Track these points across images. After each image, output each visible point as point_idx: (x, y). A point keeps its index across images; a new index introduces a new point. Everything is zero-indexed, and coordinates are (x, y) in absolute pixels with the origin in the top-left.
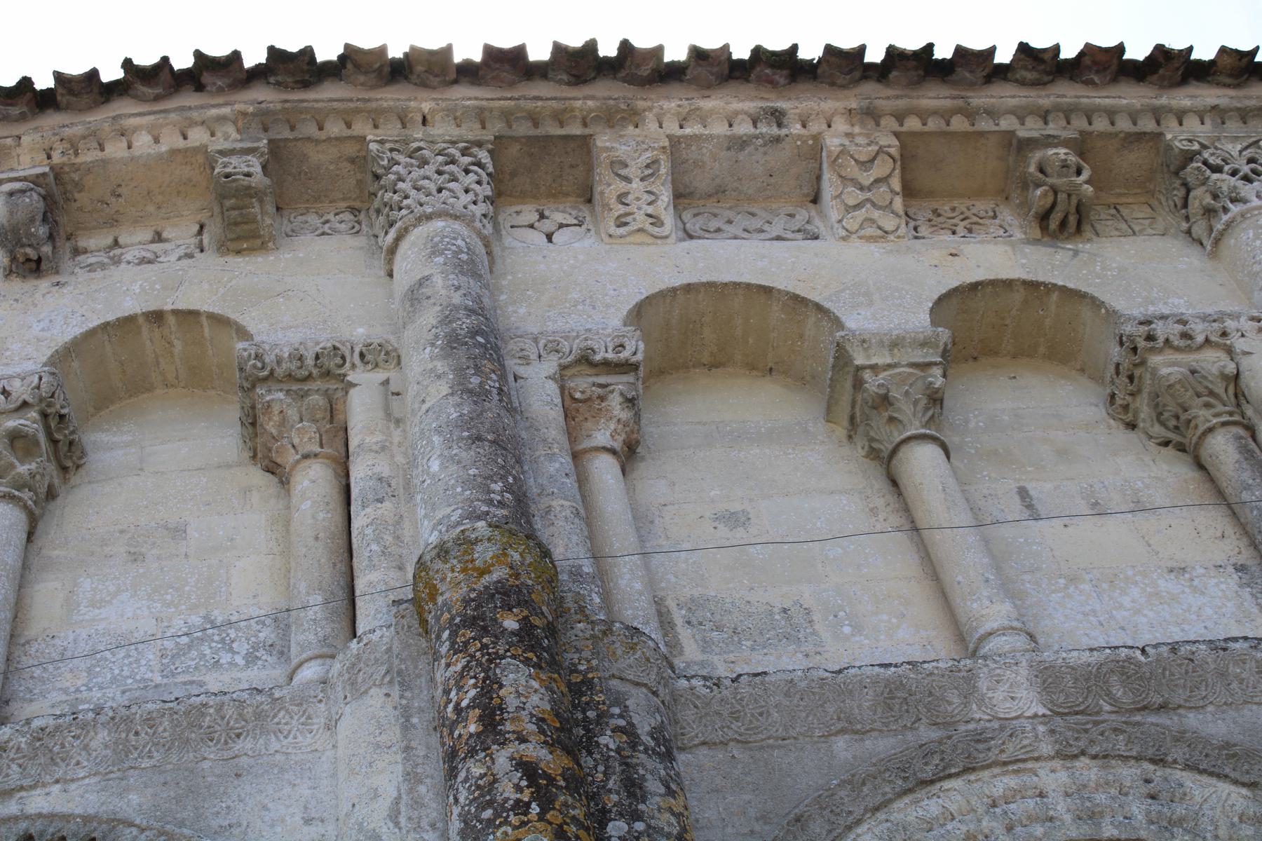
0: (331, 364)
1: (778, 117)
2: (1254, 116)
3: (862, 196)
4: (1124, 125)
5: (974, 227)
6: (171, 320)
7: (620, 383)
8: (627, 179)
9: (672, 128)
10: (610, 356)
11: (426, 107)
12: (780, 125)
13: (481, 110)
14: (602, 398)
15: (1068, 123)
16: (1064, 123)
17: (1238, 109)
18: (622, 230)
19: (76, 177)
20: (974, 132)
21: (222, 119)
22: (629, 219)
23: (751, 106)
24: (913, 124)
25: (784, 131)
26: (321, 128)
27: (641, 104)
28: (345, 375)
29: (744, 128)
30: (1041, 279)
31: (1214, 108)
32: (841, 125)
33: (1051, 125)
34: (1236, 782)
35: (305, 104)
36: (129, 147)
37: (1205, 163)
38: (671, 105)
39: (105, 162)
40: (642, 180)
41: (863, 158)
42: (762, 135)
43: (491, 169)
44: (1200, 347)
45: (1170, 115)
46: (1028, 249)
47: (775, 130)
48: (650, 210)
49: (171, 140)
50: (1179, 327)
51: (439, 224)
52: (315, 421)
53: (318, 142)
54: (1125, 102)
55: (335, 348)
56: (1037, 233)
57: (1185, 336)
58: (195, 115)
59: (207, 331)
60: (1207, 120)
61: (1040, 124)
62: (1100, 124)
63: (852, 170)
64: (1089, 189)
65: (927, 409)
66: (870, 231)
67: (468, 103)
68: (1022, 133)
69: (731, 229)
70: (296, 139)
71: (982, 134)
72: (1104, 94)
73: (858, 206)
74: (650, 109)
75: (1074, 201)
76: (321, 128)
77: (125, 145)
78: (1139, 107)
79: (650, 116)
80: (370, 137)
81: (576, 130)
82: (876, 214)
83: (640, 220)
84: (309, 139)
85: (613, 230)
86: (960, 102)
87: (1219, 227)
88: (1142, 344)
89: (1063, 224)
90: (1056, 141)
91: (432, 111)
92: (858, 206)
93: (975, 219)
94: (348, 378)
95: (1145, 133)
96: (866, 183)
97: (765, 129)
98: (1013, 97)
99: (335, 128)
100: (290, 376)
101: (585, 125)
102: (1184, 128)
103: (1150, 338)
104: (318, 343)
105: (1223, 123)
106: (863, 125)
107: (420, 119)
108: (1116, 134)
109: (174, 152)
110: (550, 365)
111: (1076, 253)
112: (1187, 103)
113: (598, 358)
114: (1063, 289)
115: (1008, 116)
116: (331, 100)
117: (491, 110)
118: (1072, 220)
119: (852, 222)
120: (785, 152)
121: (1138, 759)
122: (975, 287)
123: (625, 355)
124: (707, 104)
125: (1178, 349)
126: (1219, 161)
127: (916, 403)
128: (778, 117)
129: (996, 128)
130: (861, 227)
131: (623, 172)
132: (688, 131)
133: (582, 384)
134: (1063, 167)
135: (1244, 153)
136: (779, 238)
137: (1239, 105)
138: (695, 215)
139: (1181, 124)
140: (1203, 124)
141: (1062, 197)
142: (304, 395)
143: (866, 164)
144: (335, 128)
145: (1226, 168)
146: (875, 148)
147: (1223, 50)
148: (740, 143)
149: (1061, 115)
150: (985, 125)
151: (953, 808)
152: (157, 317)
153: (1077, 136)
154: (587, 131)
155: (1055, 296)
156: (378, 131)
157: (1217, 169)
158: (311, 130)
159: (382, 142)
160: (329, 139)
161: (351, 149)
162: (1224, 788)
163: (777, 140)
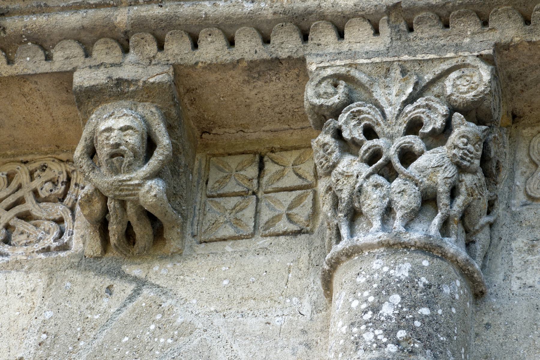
2: (459, 16)
5: (21, 225)
15: (161, 47)
16: (152, 48)
20: (12, 77)
37: (338, 134)
45: (322, 23)
60: (385, 30)
71: (24, 78)
75: (131, 211)
78: (270, 17)
90: (132, 88)
95: (278, 61)
102: (345, 46)
105: (411, 29)
108: (235, 64)
115: (66, 43)
129: (45, 67)
134: (112, 156)
135: (409, 108)
139: (341, 35)
140: (377, 32)
149: (149, 37)
153: (164, 78)
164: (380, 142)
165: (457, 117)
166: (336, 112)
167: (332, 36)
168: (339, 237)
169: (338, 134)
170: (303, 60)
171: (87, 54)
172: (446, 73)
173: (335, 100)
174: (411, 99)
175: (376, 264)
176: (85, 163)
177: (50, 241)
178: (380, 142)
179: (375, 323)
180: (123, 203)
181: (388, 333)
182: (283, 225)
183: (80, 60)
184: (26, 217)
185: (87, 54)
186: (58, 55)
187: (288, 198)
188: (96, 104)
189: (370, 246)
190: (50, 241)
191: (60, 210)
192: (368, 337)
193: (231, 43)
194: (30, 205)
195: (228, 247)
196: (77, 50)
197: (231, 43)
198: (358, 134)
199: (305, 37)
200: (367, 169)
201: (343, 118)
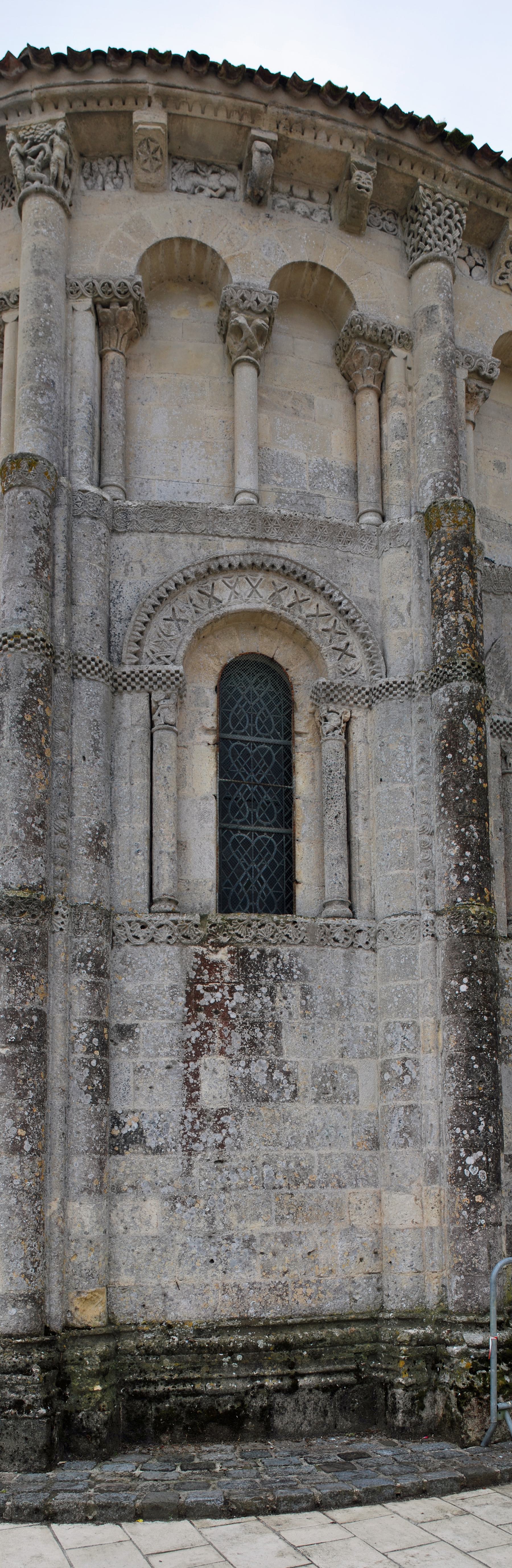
6: (319, 269)
13: (469, 182)
14: (477, 394)
19: (286, 145)
21: (360, 139)
22: (505, 276)
28: (390, 347)
35: (398, 145)
36: (315, 138)
39: (302, 143)
49: (334, 144)
51: (442, 266)
55: (390, 330)
58: (350, 130)
59: (331, 283)
67: (466, 175)
70: (388, 167)
77: (313, 136)
84: (394, 170)
85: (497, 280)
91: (450, 173)
99: (406, 168)
100: (370, 340)
101: (507, 210)
104: (384, 324)
107: (442, 176)
109: (335, 151)
113: (483, 373)
117: (473, 184)
142: (372, 351)
152: (314, 266)
158: (395, 163)
159: (425, 187)
160: (402, 173)
161: (408, 182)
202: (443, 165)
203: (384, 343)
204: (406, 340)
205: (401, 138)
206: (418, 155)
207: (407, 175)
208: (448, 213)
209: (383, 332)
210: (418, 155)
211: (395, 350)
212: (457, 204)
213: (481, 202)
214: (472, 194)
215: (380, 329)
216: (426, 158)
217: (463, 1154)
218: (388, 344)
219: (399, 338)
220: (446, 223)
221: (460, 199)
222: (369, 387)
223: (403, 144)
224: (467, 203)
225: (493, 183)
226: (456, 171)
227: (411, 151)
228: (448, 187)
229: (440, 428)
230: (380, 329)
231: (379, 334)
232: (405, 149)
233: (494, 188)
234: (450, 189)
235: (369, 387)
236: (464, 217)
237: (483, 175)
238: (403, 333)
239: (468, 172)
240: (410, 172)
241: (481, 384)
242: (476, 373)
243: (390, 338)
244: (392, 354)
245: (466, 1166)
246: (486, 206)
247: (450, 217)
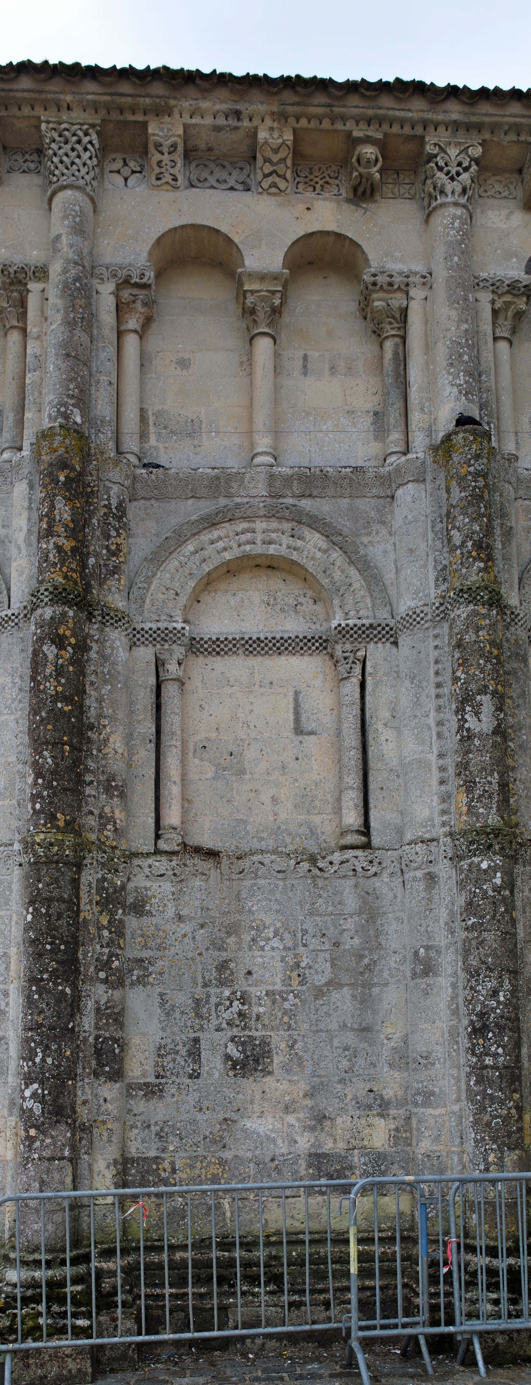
0: (21, 276)
1: (238, 115)
3: (272, 169)
4: (407, 130)
5: (326, 186)
7: (141, 294)
8: (163, 154)
9: (187, 119)
10: (138, 280)
11: (69, 98)
12: (239, 120)
14: (134, 302)
16: (377, 126)
17: (466, 123)
18: (159, 183)
23: (224, 107)
24: (303, 122)
25: (240, 124)
26: (20, 109)
27: (172, 102)
28: (26, 284)
29: (221, 121)
30: (342, 232)
31: (455, 122)
32: (268, 122)
33: (371, 127)
34: (322, 534)
35: (11, 94)
37: (437, 164)
38: (186, 104)
40: (169, 153)
41: (274, 147)
42: (229, 126)
43: (97, 146)
44: (396, 291)
46: (345, 206)
47: (235, 123)
48: (172, 171)
50: (388, 279)
52: (15, 307)
53: (18, 118)
54: (410, 114)
56: (351, 196)
57: (391, 284)
60: (449, 129)
61: (366, 126)
62: (396, 129)
63: (269, 154)
64: (377, 176)
65: (270, 316)
66: (273, 190)
67: (90, 97)
68: (356, 134)
69: (212, 180)
71: (336, 131)
72: (403, 106)
73: (270, 174)
74: (176, 106)
76: (20, 109)
79: (176, 111)
80: (42, 118)
81: (140, 118)
82: (277, 180)
83: (168, 178)
84: (14, 116)
86: (327, 110)
87: (434, 204)
88: (370, 287)
89: (364, 193)
91: (72, 101)
92: (270, 174)
93: (327, 179)
94: (28, 287)
96: (275, 160)
97: (232, 122)
98: (356, 107)
99: (26, 111)
101: (145, 114)
102: (437, 134)
103: (374, 284)
106: (279, 122)
107: (66, 106)
110: (110, 287)
111: (366, 209)
112: (441, 117)
113: (132, 281)
114: (351, 240)
116: (24, 91)
117: (100, 102)
118: (368, 191)
119: (265, 184)
120: (240, 135)
121: (293, 520)
122: (312, 234)
123: (144, 281)
124: (205, 105)
125: (385, 291)
126: (443, 165)
127: (266, 313)
128: (238, 115)
129: (343, 128)
130: (270, 187)
131: (160, 149)
132: (194, 121)
133: (126, 294)
136: (232, 189)
137: (467, 121)
138: (197, 166)
141: (364, 180)
143: (276, 151)
144: (26, 111)
145: (446, 169)
146: (280, 141)
147: (465, 87)
148: (218, 129)
150: (339, 126)
151: (222, 535)
153: (381, 137)
154: (146, 118)
155: (348, 241)
156: (47, 113)
157: (440, 169)
158: (15, 111)
159: (48, 122)
160: (24, 117)
161: (34, 122)
162: (317, 535)
163: (237, 128)
164: (449, 168)
165: (473, 163)
166: (436, 156)
167: (433, 129)
168: (436, 199)
169: (437, 164)
170: (423, 137)
171: (357, 125)
172: (468, 147)
173: (435, 152)
174: (458, 155)
175: (451, 209)
176: (356, 164)
177: (336, 192)
178: (449, 168)
179: (453, 228)
180: (367, 180)
181: (458, 232)
182: (407, 195)
183: (354, 127)
184: (327, 183)
185: (357, 125)
186: (348, 124)
187: (408, 187)
188: (358, 144)
189: (449, 203)
190: (336, 192)
191: (337, 182)
192: (452, 233)
193: (402, 127)
194: (327, 179)
195: (391, 201)
196: (354, 123)
197: (402, 127)
198: (443, 165)
199: (425, 129)
200: (446, 177)
201: (439, 158)
202: (62, 97)
203: (20, 282)
204: (41, 273)
205: (15, 86)
206: (33, 95)
207: (29, 117)
208: (75, 139)
209: (16, 272)
210: (33, 95)
211: (31, 286)
212: (85, 127)
213: (115, 116)
214: (103, 112)
215: (12, 270)
216: (43, 96)
217: (23, 1087)
218: (24, 281)
219: (34, 273)
220: (73, 149)
221: (90, 121)
222: (12, 327)
223: (17, 91)
224: (99, 122)
225: (122, 95)
226: (77, 97)
227: (26, 95)
228: (74, 114)
229: (57, 355)
230: (12, 270)
231: (12, 276)
232: (19, 95)
233: (123, 99)
234: (77, 115)
235: (12, 327)
236: (94, 137)
237: (109, 91)
238: (36, 267)
239: (93, 93)
240: (32, 113)
241: (135, 291)
242: (126, 282)
243: (24, 275)
244: (28, 291)
245: (24, 1099)
246: (121, 118)
247: (79, 142)
